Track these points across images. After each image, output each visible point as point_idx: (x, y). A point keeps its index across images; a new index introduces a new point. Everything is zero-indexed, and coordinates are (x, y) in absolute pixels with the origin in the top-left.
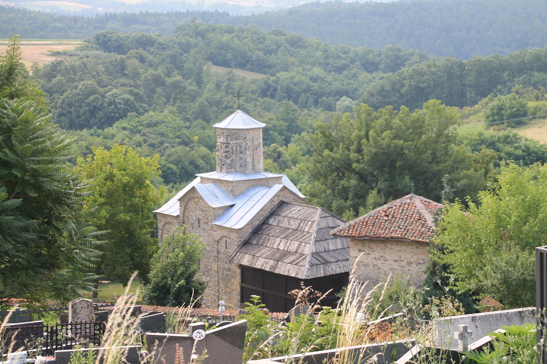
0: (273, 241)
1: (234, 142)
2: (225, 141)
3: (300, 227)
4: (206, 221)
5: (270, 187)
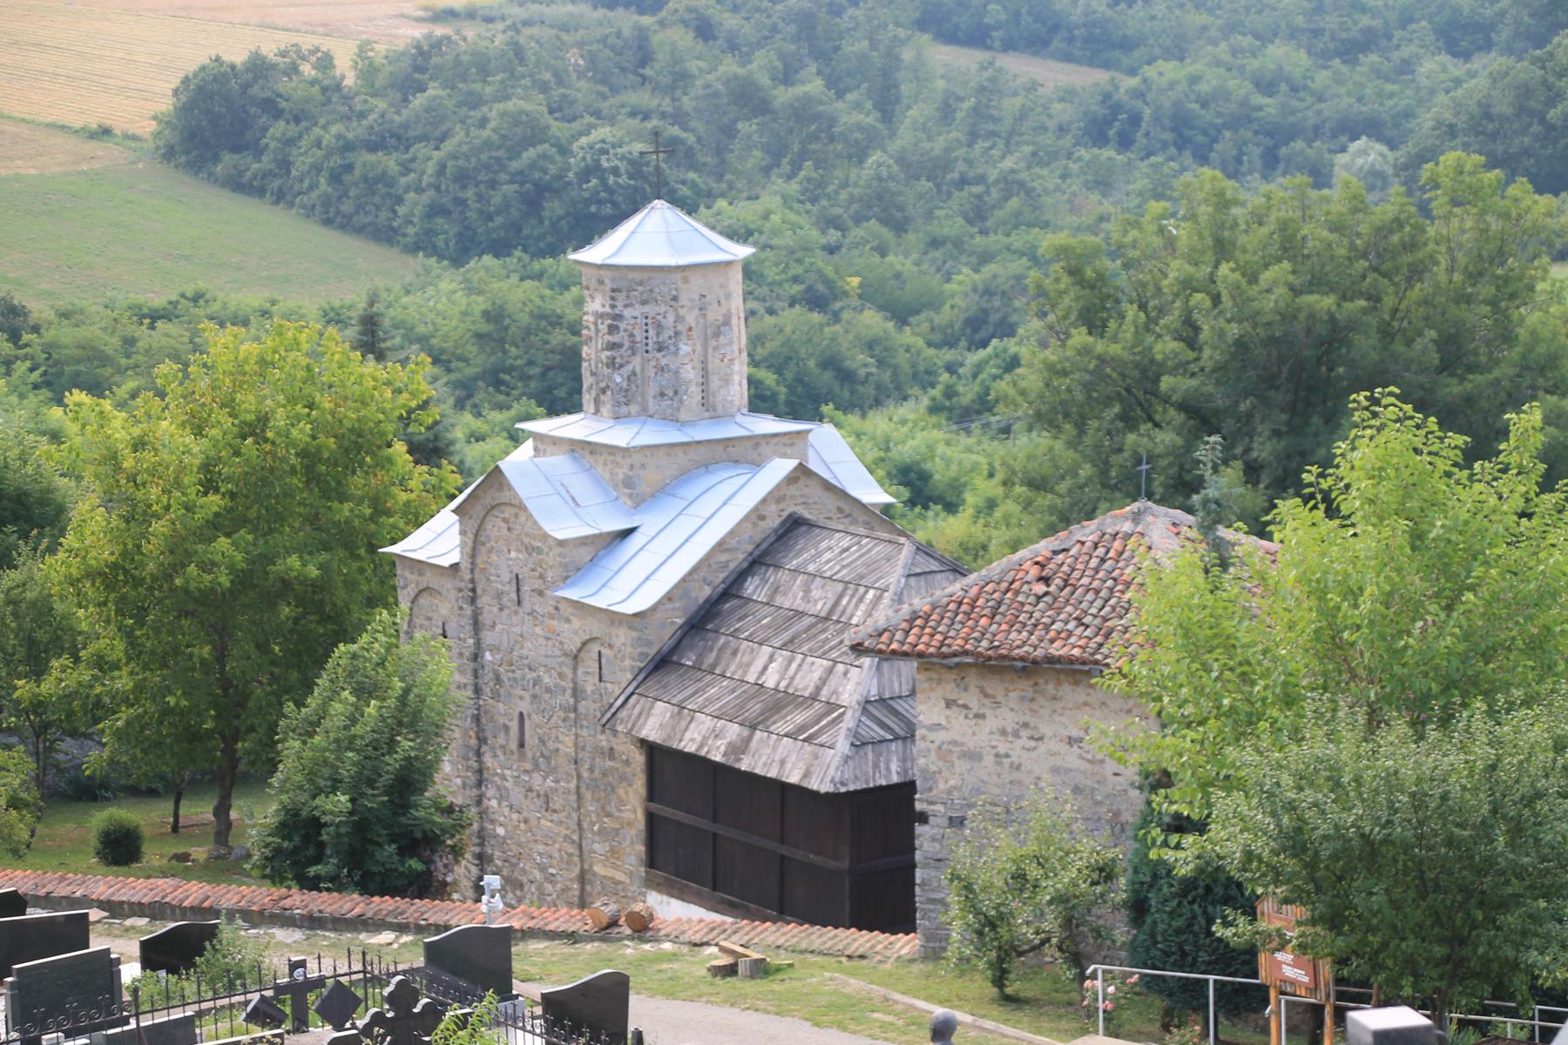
0: (746, 659)
1: (638, 310)
2: (608, 309)
3: (840, 608)
4: (538, 584)
5: (757, 464)
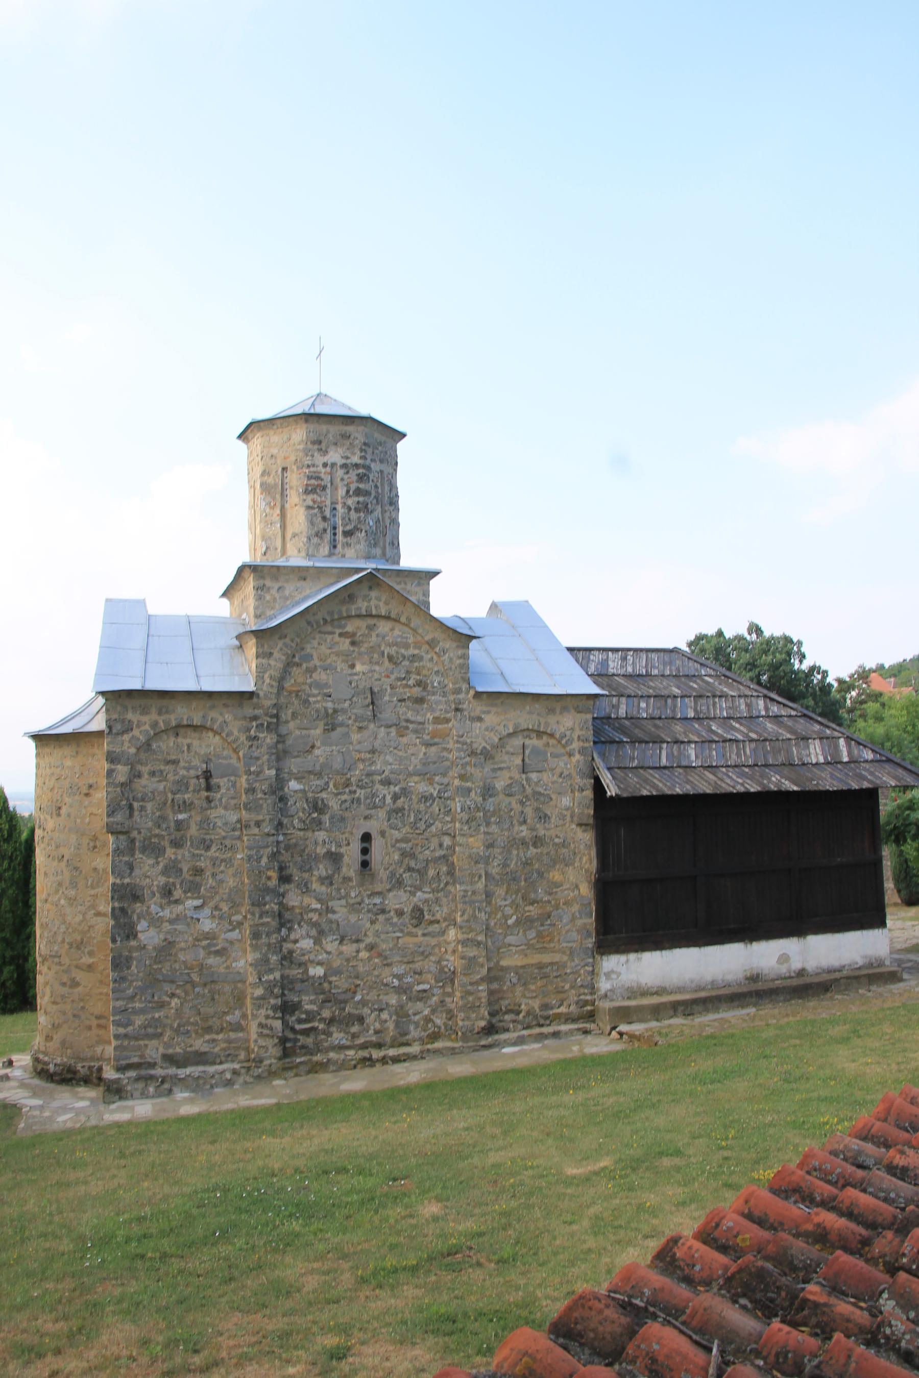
2: (356, 459)
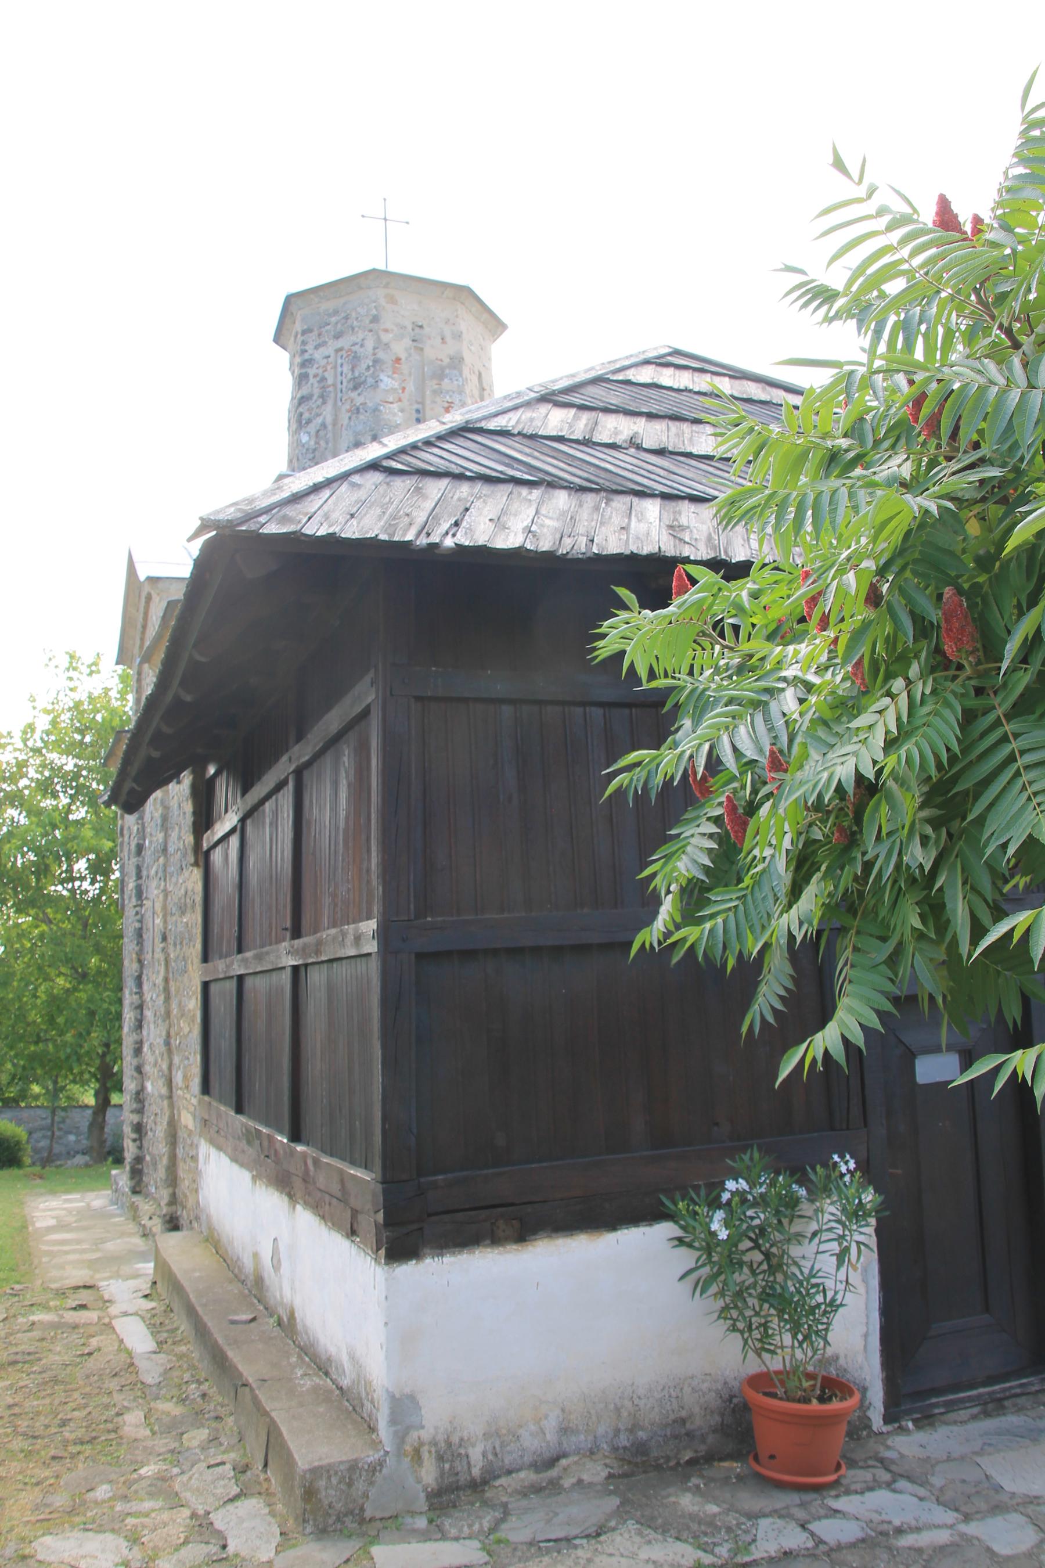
1: (332, 346)
